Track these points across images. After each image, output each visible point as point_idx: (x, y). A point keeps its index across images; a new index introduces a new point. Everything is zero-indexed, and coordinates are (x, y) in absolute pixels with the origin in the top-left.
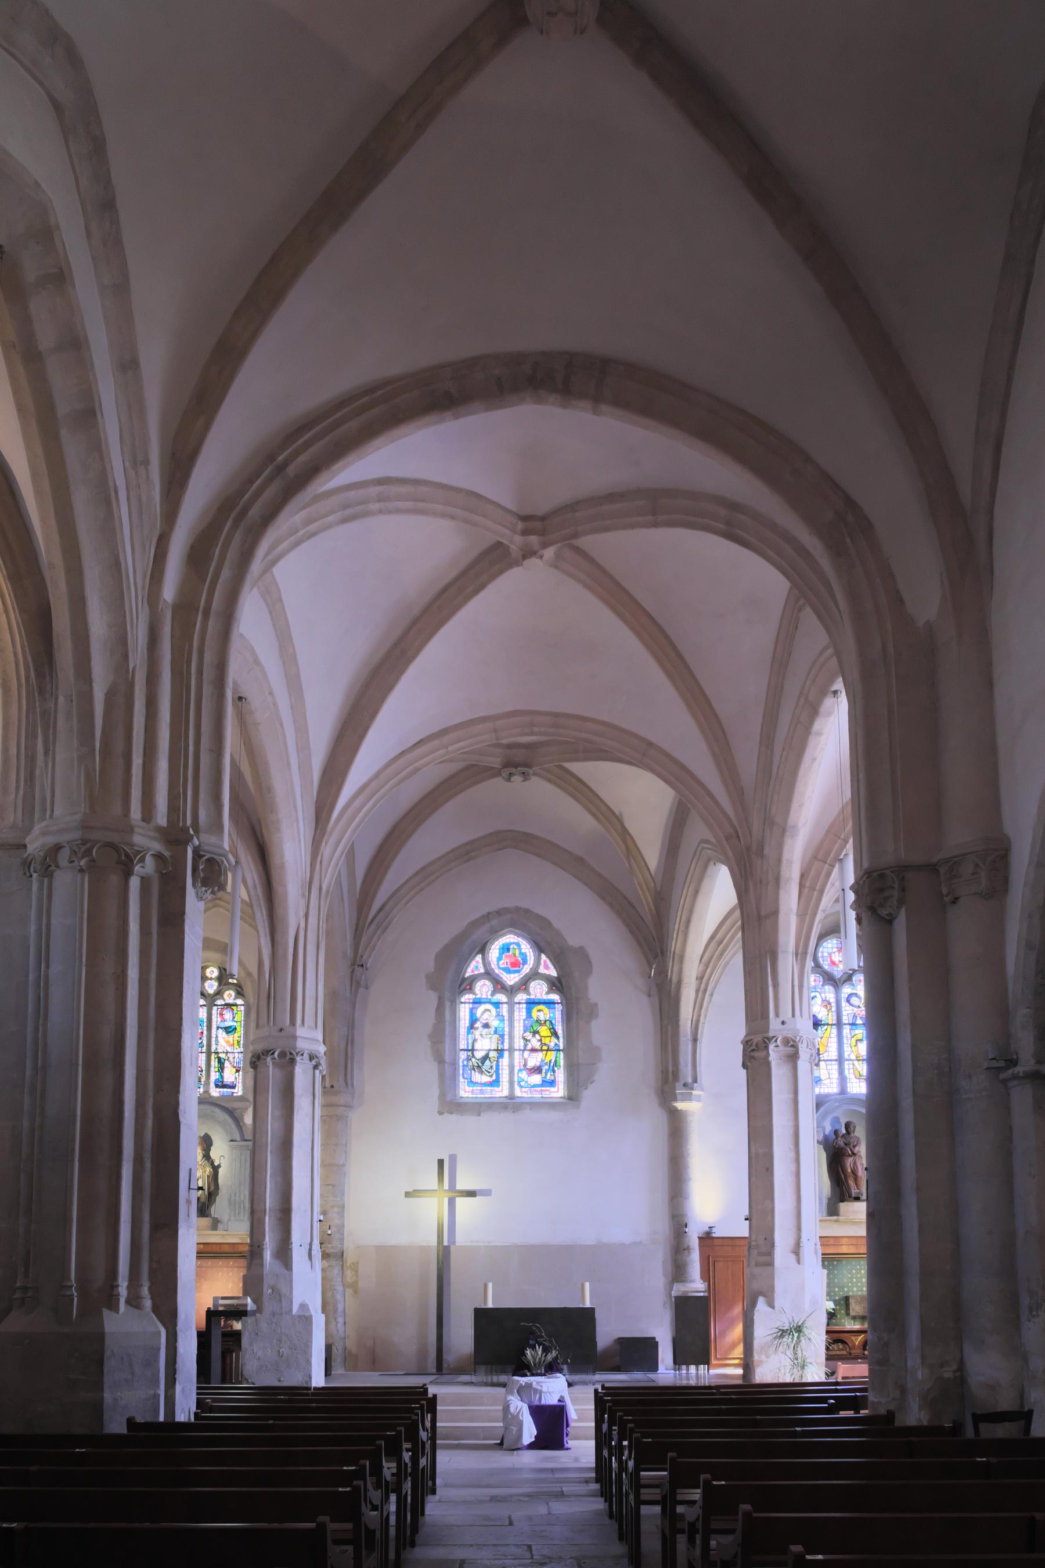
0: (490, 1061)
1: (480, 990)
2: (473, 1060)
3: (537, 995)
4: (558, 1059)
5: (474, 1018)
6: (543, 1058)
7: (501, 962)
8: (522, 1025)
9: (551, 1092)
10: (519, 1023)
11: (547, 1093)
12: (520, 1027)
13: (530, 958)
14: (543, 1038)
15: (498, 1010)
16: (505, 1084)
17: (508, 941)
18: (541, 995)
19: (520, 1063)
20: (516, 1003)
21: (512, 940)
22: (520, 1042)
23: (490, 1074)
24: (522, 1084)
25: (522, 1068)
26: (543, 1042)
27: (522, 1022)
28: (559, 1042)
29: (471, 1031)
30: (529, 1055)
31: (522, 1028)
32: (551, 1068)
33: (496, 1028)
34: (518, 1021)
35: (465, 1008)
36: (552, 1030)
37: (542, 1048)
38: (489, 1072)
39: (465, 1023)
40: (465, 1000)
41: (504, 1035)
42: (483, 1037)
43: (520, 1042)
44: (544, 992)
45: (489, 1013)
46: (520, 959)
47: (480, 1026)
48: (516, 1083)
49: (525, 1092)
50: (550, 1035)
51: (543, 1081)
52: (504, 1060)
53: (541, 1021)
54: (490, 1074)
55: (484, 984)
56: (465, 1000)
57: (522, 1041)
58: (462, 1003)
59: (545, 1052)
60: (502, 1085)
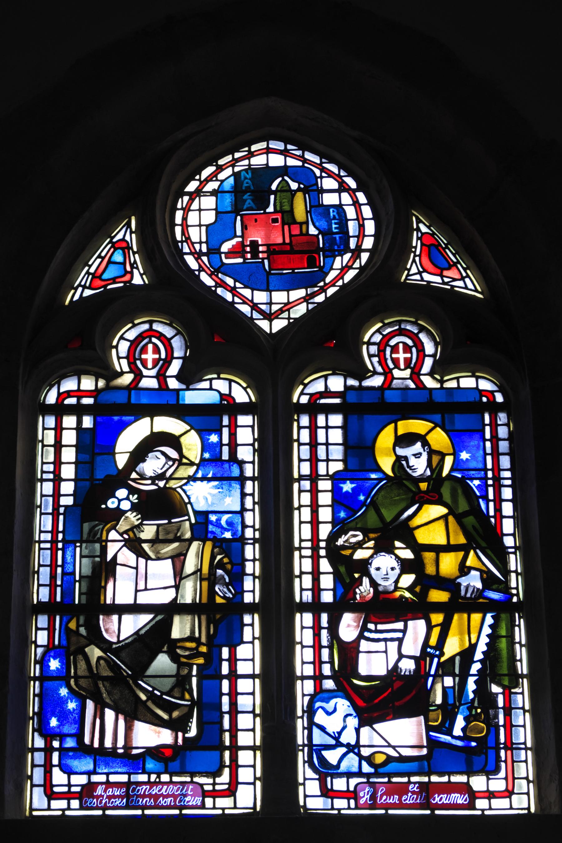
0: (175, 658)
1: (131, 358)
2: (95, 653)
3: (396, 373)
4: (503, 644)
5: (100, 475)
6: (433, 641)
7: (226, 247)
8: (325, 499)
9: (473, 795)
10: (314, 492)
11: (459, 798)
12: (315, 507)
13: (362, 227)
14: (429, 556)
15: (214, 438)
16: (245, 757)
17: (258, 161)
18: (416, 375)
19: (317, 662)
20: (300, 409)
21: (276, 161)
22: (316, 574)
23: (175, 714)
24: (332, 756)
25: (329, 684)
26: (430, 570)
27: (325, 485)
28: (506, 572)
29: (86, 526)
30: (364, 628)
31: (325, 514)
32: (471, 685)
33: (203, 515)
34: (306, 485)
35: (59, 429)
36: (470, 520)
37: (424, 594)
38: (169, 707)
39: (57, 495)
40: (62, 396)
41: (242, 541)
42: (140, 553)
43: (316, 574)
44: (428, 363)
45: (174, 454)
46: (313, 231)
47: (126, 505)
48: (301, 757)
49: (340, 795)
50: (462, 540)
51: (432, 743)
52: (243, 651)
53: (417, 481)
54: (175, 714)
55: (150, 333)
56: (62, 396)
57: (325, 565)
58: (47, 410)
59: (437, 618)
60: (235, 766)
